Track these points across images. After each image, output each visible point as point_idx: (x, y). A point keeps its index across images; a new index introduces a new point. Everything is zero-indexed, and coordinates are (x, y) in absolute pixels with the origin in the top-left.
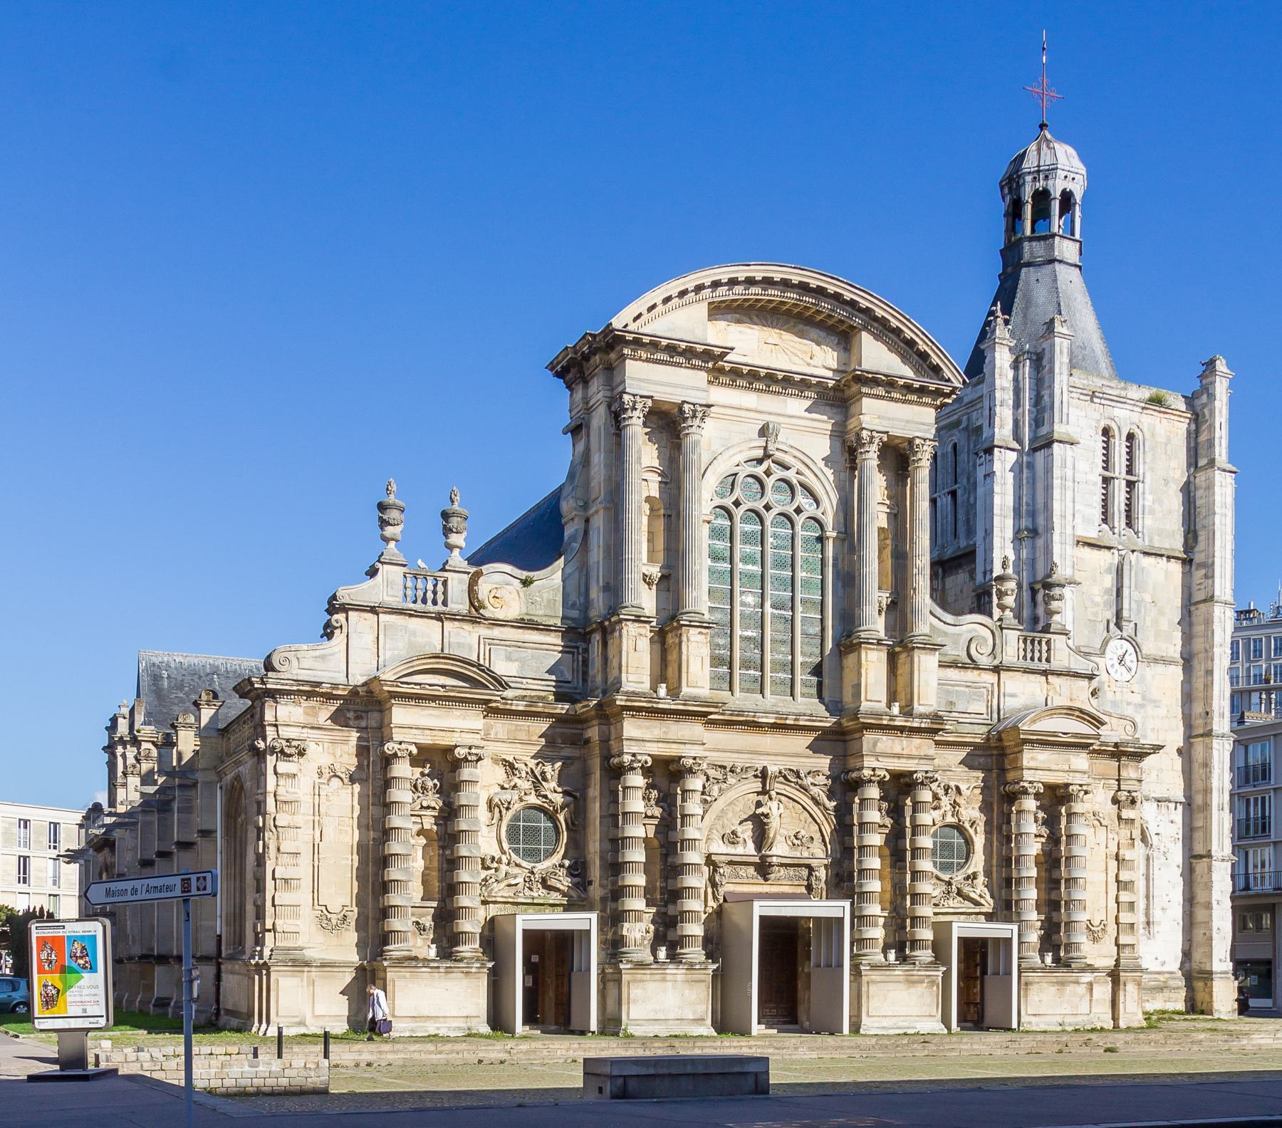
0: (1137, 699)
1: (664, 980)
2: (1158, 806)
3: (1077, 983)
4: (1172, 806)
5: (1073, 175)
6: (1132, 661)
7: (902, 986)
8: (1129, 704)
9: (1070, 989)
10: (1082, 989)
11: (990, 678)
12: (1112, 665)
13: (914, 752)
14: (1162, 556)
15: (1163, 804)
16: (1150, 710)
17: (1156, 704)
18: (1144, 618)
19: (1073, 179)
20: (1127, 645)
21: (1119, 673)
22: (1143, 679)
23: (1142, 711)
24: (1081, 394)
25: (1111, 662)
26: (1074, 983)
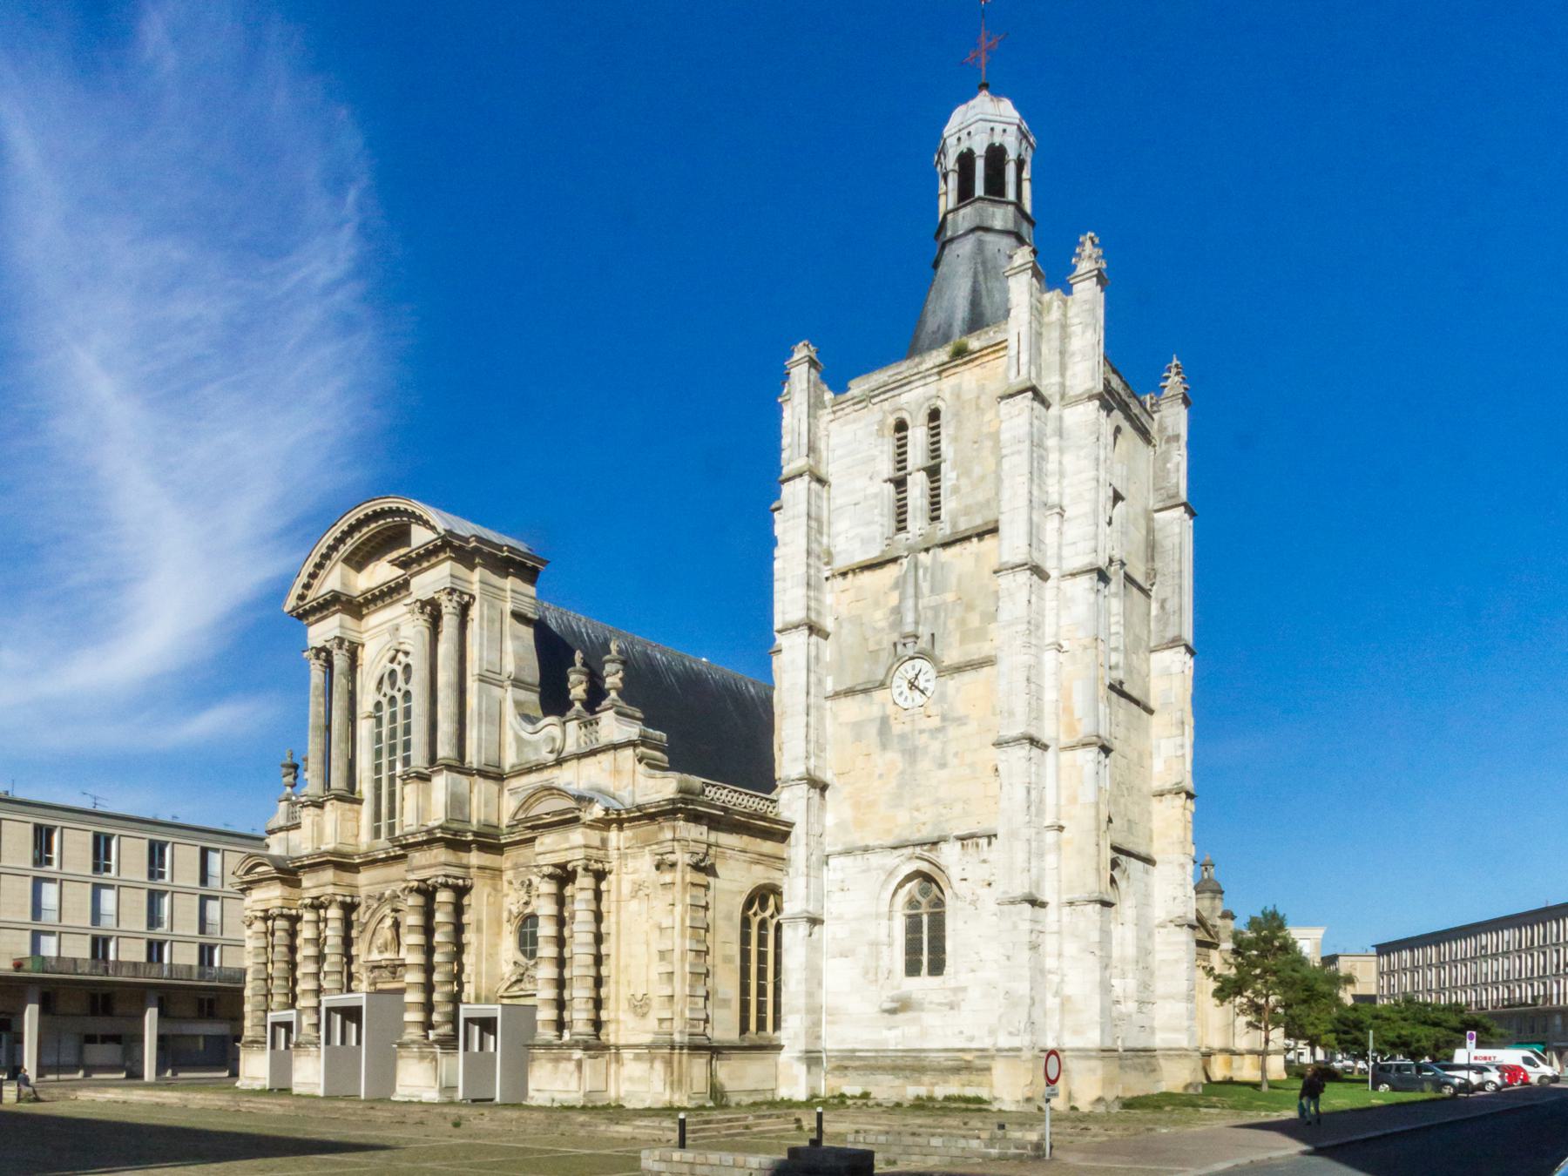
0: (935, 722)
1: (309, 1055)
2: (963, 845)
3: (569, 1059)
4: (984, 841)
5: (966, 131)
6: (928, 681)
7: (415, 1061)
8: (921, 732)
9: (563, 1065)
10: (571, 1066)
11: (556, 772)
12: (901, 694)
13: (433, 862)
14: (968, 538)
15: (970, 842)
16: (953, 731)
17: (961, 721)
18: (945, 624)
19: (969, 134)
20: (919, 663)
21: (910, 700)
22: (942, 697)
23: (940, 736)
24: (854, 404)
25: (898, 691)
26: (565, 1059)
